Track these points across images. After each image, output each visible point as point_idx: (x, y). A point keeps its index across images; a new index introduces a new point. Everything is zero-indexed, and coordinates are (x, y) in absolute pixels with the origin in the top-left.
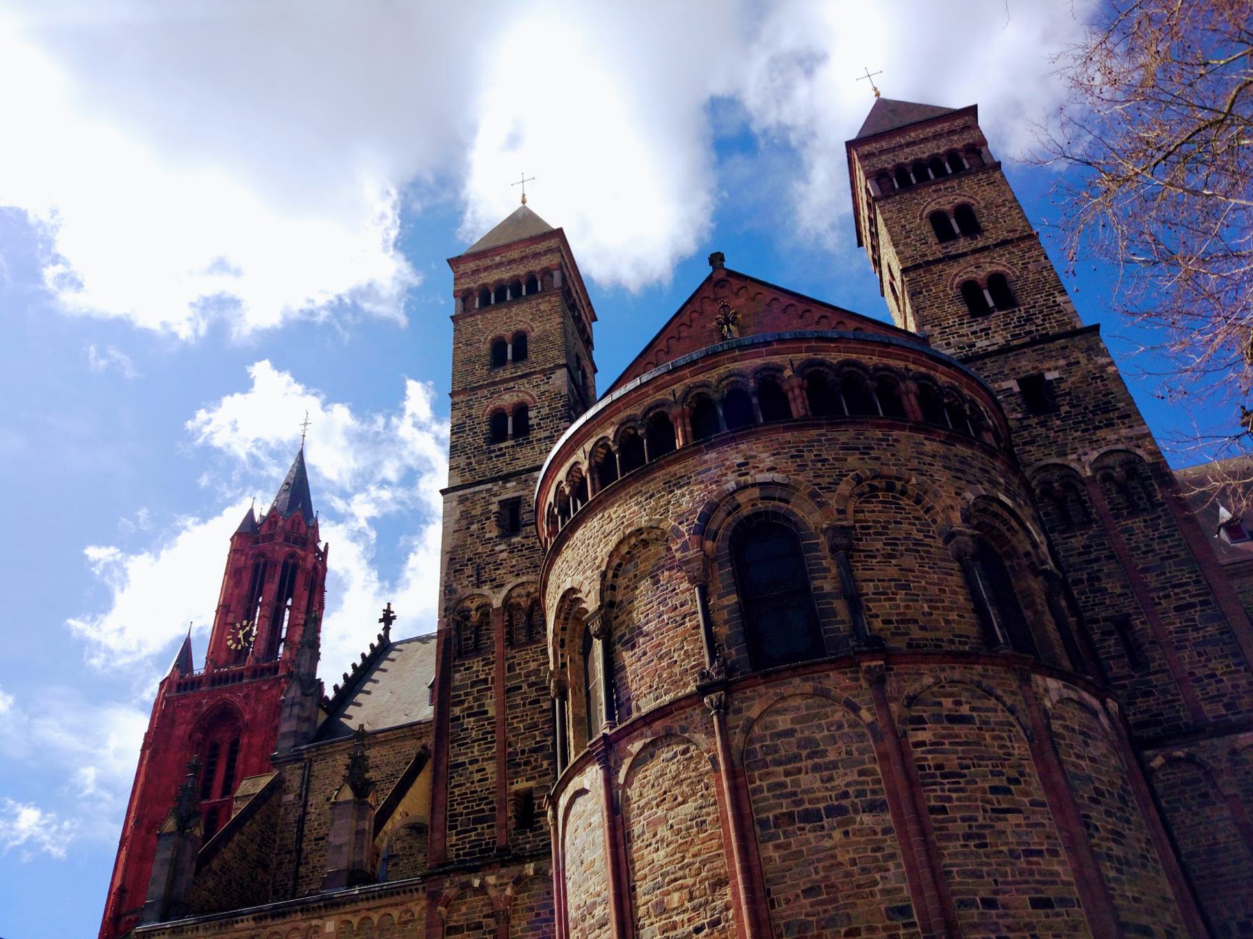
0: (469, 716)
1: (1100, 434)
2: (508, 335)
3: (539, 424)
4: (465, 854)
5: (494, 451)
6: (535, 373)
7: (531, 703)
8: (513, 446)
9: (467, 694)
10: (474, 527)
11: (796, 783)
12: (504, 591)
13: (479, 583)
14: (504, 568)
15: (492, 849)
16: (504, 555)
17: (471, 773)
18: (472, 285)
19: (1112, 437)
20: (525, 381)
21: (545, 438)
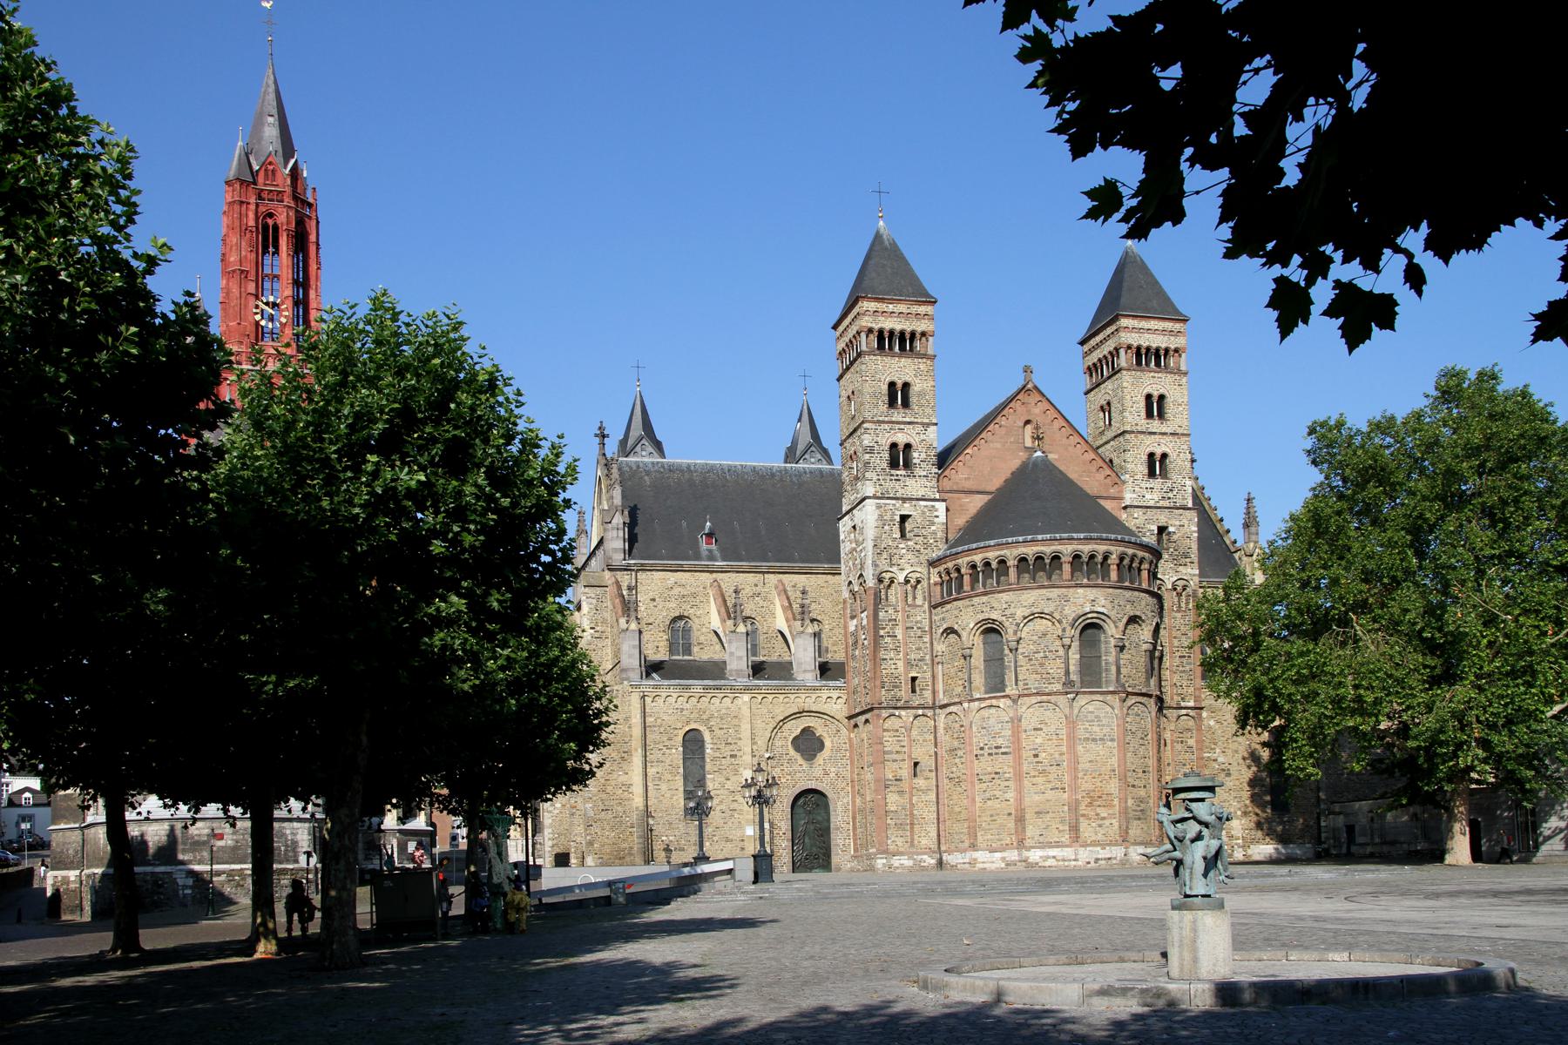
6: (917, 423)
10: (886, 527)
12: (905, 573)
13: (892, 565)
18: (873, 325)
20: (911, 427)
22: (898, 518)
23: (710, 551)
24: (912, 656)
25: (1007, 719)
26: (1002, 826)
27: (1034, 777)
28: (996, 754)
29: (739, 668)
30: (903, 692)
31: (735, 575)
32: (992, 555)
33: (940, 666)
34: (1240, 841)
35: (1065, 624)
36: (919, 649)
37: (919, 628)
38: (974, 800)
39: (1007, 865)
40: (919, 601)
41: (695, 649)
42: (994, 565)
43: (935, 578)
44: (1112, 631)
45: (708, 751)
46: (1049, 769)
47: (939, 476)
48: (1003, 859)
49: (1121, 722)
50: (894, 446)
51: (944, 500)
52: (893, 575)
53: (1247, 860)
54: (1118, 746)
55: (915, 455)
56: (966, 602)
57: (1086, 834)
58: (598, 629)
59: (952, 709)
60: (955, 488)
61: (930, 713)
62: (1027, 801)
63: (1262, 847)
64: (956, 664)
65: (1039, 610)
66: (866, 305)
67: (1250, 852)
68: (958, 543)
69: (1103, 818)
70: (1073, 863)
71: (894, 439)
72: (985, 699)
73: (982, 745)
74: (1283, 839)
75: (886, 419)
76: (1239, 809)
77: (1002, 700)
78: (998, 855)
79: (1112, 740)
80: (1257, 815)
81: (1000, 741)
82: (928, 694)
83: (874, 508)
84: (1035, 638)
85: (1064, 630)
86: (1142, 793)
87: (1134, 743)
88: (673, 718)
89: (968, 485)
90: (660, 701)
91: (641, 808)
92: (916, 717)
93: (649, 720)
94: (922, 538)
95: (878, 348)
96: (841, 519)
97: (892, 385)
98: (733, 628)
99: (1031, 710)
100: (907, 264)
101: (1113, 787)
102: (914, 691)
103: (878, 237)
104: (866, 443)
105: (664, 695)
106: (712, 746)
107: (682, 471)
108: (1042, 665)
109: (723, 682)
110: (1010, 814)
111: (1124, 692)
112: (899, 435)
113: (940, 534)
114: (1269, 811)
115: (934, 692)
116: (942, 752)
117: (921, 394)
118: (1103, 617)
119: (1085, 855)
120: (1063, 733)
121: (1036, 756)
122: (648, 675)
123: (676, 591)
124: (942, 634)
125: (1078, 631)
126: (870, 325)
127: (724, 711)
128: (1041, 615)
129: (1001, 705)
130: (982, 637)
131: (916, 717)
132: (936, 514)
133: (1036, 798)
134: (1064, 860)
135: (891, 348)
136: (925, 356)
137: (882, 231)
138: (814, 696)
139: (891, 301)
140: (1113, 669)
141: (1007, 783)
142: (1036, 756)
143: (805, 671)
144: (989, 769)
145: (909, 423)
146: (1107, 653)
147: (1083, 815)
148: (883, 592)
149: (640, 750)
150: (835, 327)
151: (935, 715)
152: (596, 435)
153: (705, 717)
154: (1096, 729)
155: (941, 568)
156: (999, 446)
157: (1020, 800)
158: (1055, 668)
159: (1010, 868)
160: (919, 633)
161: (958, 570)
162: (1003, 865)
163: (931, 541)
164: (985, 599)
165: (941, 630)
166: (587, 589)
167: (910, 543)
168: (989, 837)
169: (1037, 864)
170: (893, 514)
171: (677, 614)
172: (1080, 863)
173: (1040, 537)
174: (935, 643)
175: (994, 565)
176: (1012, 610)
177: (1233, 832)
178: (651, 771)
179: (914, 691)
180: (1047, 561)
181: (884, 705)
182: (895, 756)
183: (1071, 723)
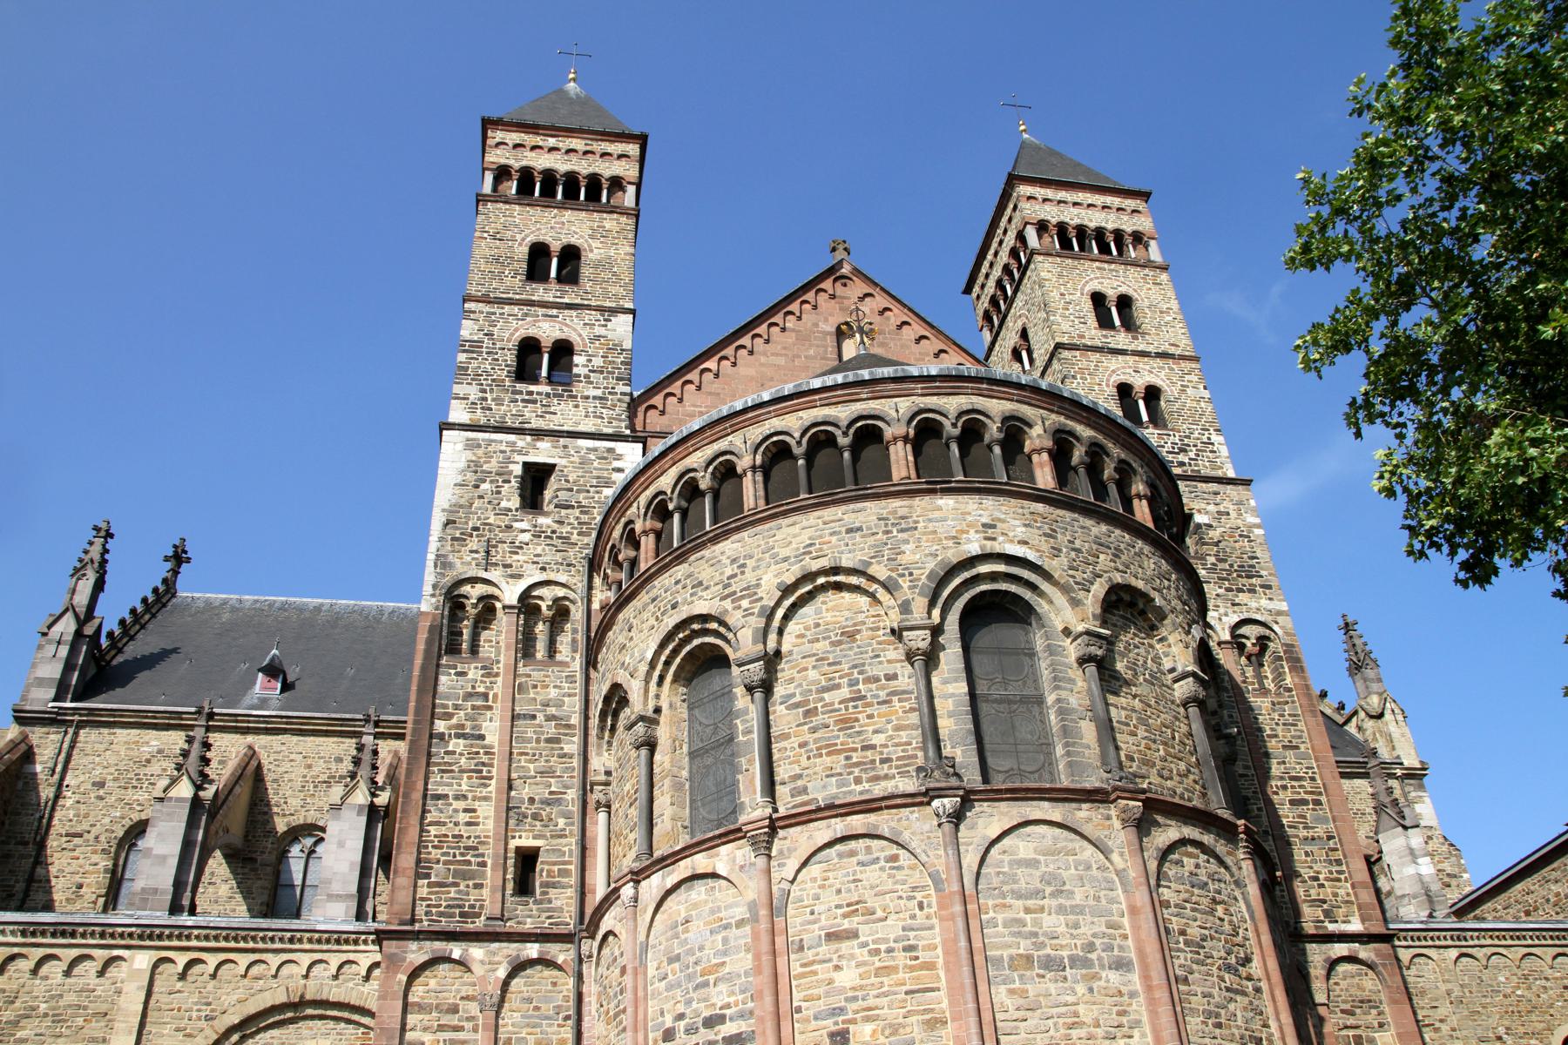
0: (458, 736)
1: (1243, 598)
2: (555, 246)
3: (587, 377)
4: (441, 914)
5: (521, 393)
6: (589, 307)
7: (548, 741)
8: (548, 395)
9: (456, 707)
10: (485, 486)
11: (1036, 922)
12: (522, 585)
14: (524, 554)
15: (478, 915)
16: (526, 537)
17: (456, 811)
18: (511, 162)
19: (1254, 605)
20: (574, 313)
21: (594, 398)
22: (517, 470)
30: (486, 892)
31: (295, 738)
33: (602, 816)
36: (547, 773)
37: (549, 718)
49: (1142, 897)
52: (490, 590)
54: (1149, 988)
65: (824, 563)
77: (724, 849)
79: (1120, 965)
81: (720, 996)
83: (460, 446)
84: (822, 646)
85: (905, 608)
87: (1204, 987)
92: (519, 967)
94: (577, 512)
99: (814, 870)
102: (524, 886)
108: (846, 723)
117: (604, 264)
120: (935, 940)
126: (503, 161)
131: (519, 967)
132: (616, 464)
143: (332, 897)
152: (167, 559)
156: (781, 361)
160: (551, 730)
167: (542, 520)
176: (750, 577)
179: (524, 886)
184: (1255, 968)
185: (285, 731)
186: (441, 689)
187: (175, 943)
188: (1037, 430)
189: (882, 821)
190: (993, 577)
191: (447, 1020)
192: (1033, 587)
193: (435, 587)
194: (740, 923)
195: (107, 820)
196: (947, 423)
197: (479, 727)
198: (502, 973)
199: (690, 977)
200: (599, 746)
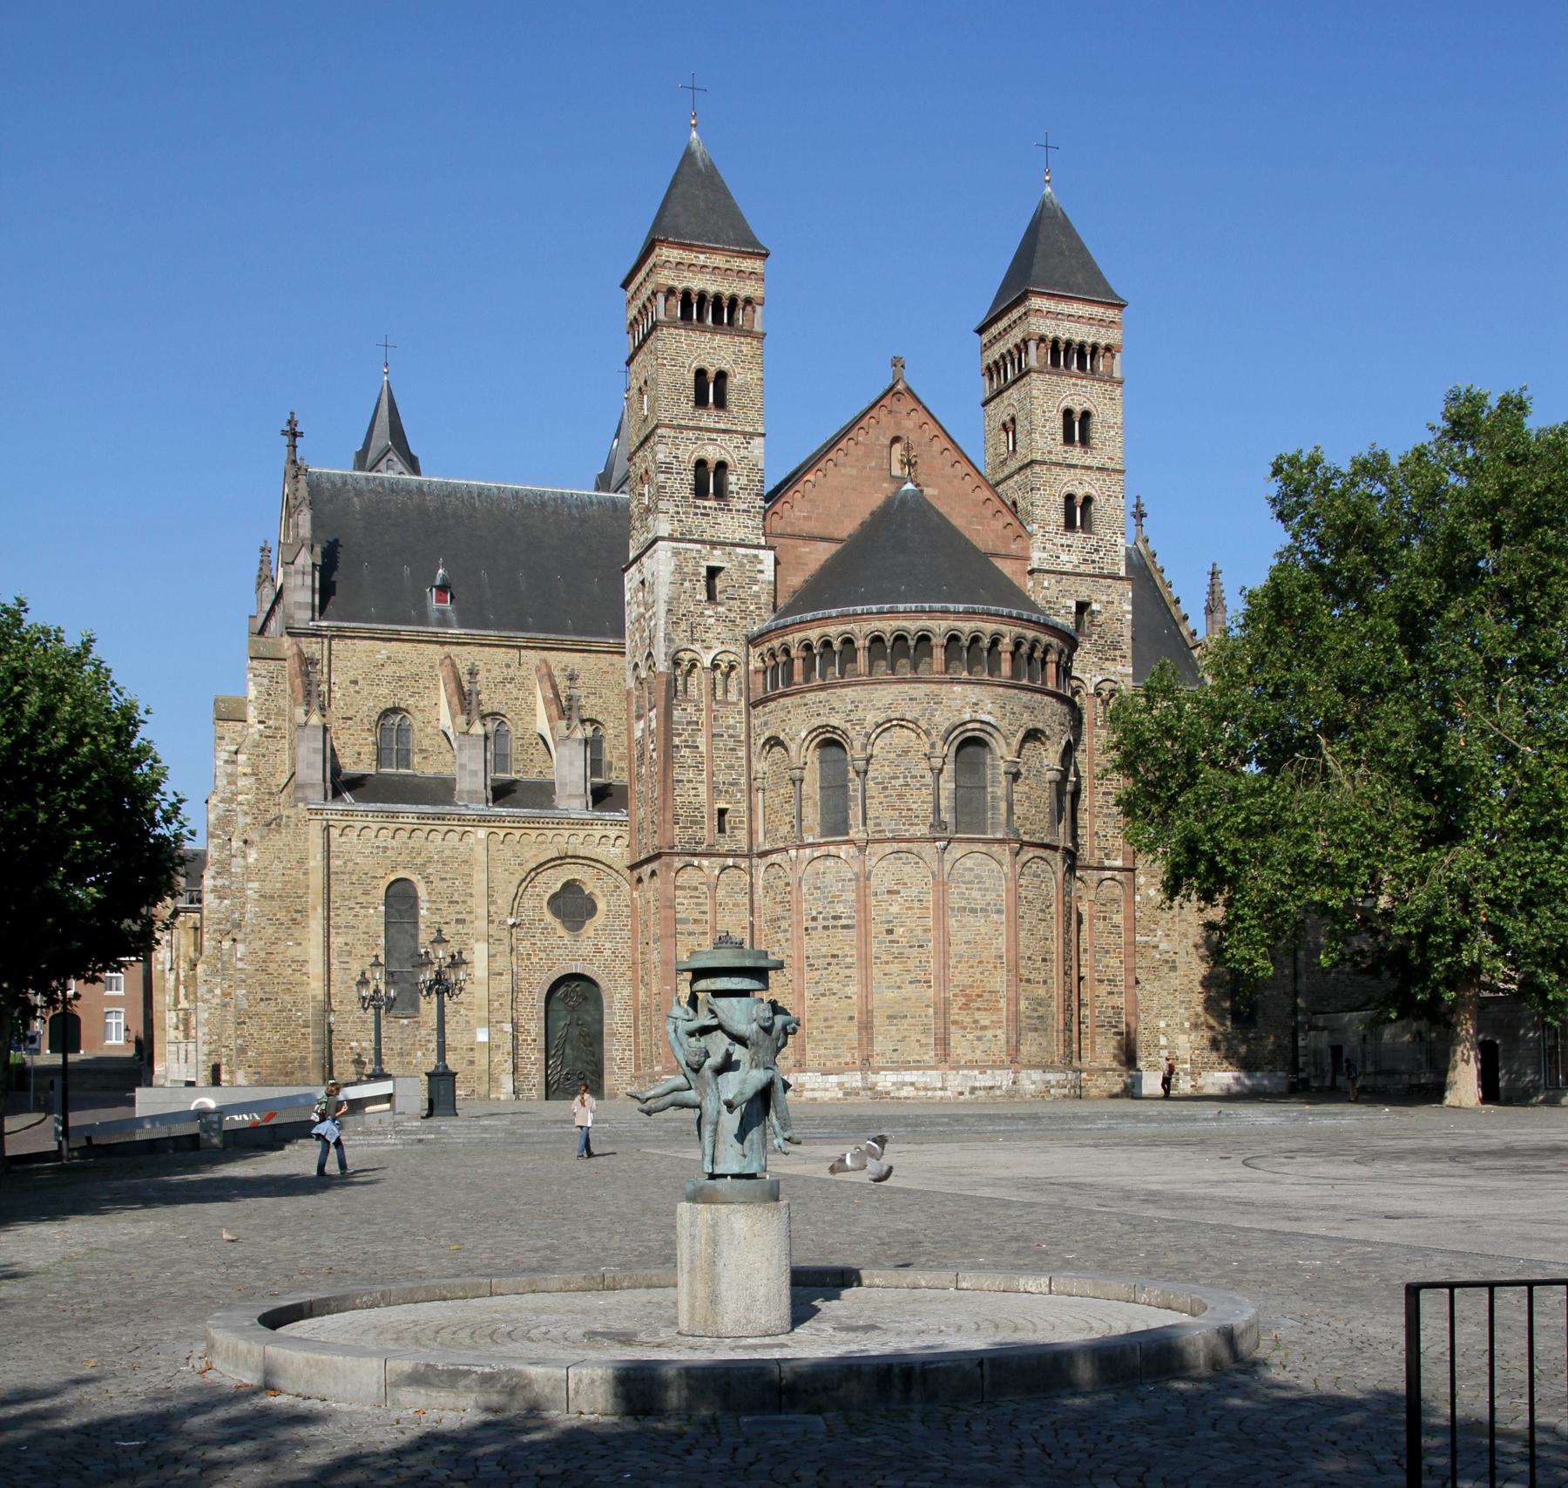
6: (736, 432)
7: (731, 750)
10: (687, 584)
12: (712, 655)
13: (693, 641)
18: (676, 284)
22: (704, 572)
23: (443, 612)
24: (721, 778)
25: (850, 875)
26: (841, 1035)
27: (887, 963)
28: (834, 927)
29: (473, 787)
30: (705, 831)
31: (477, 649)
32: (833, 630)
33: (760, 794)
34: (1188, 1066)
35: (934, 738)
36: (730, 767)
37: (731, 736)
38: (802, 996)
39: (846, 1094)
40: (733, 697)
41: (416, 759)
42: (837, 645)
43: (756, 663)
44: (1002, 751)
45: (423, 912)
46: (907, 951)
47: (766, 511)
48: (841, 1085)
49: (1011, 885)
50: (701, 464)
51: (771, 548)
52: (695, 656)
53: (1196, 1094)
54: (1008, 921)
55: (732, 478)
56: (796, 699)
57: (959, 1051)
58: (271, 723)
59: (774, 858)
60: (789, 530)
61: (744, 863)
62: (876, 1000)
63: (1218, 1074)
64: (782, 791)
65: (897, 715)
66: (665, 253)
67: (1200, 1082)
68: (791, 610)
69: (984, 1028)
70: (940, 1093)
71: (702, 454)
72: (820, 845)
73: (814, 914)
74: (1247, 1065)
75: (691, 424)
76: (1188, 1019)
78: (833, 1079)
79: (999, 912)
80: (1211, 1028)
82: (742, 835)
83: (669, 554)
85: (933, 746)
86: (1041, 991)
87: (1031, 917)
88: (371, 861)
89: (810, 527)
90: (353, 835)
91: (321, 997)
93: (336, 863)
94: (738, 602)
95: (683, 318)
96: (625, 570)
97: (701, 374)
98: (465, 728)
99: (884, 863)
100: (729, 196)
101: (999, 981)
102: (721, 830)
103: (689, 155)
104: (660, 457)
105: (359, 825)
106: (428, 905)
107: (409, 492)
108: (900, 796)
109: (447, 809)
110: (851, 1018)
111: (1016, 841)
112: (710, 448)
113: (764, 598)
114: (1229, 1023)
115: (751, 833)
116: (760, 922)
117: (744, 389)
118: (989, 729)
119: (956, 1082)
121: (890, 932)
122: (337, 794)
123: (389, 670)
124: (764, 745)
125: (953, 749)
126: (670, 283)
127: (448, 853)
128: (902, 722)
129: (842, 855)
130: (817, 752)
131: (724, 869)
132: (760, 567)
133: (890, 994)
134: (926, 1089)
135: (701, 318)
136: (749, 333)
137: (694, 145)
138: (582, 834)
139: (703, 249)
140: (1003, 806)
141: (848, 972)
142: (890, 932)
143: (570, 796)
144: (824, 950)
145: (725, 431)
146: (995, 782)
147: (955, 1022)
148: (680, 681)
149: (320, 909)
150: (625, 285)
151: (751, 866)
152: (284, 433)
153: (419, 861)
154: (976, 894)
155: (764, 648)
156: (854, 472)
157: (866, 996)
158: (920, 802)
159: (851, 1099)
160: (731, 744)
161: (787, 652)
162: (840, 1095)
163: (752, 608)
164: (822, 695)
165: (762, 741)
166: (255, 663)
167: (721, 609)
168: (823, 1051)
169: (888, 1093)
170: (698, 565)
171: (389, 705)
172: (949, 1093)
173: (901, 607)
174: (754, 760)
175: (837, 645)
176: (860, 714)
177: (1178, 1053)
178: (337, 941)
179: (721, 830)
180: (912, 643)
181: (678, 849)
182: (691, 927)
183: (941, 884)
184: (1053, 908)
185: (469, 644)
186: (675, 719)
187: (497, 824)
188: (1007, 640)
189: (914, 847)
190: (974, 730)
191: (693, 893)
192: (991, 735)
193: (666, 654)
194: (850, 880)
195: (365, 708)
196: (963, 638)
197: (694, 741)
198: (717, 872)
199: (825, 898)
200: (759, 758)
